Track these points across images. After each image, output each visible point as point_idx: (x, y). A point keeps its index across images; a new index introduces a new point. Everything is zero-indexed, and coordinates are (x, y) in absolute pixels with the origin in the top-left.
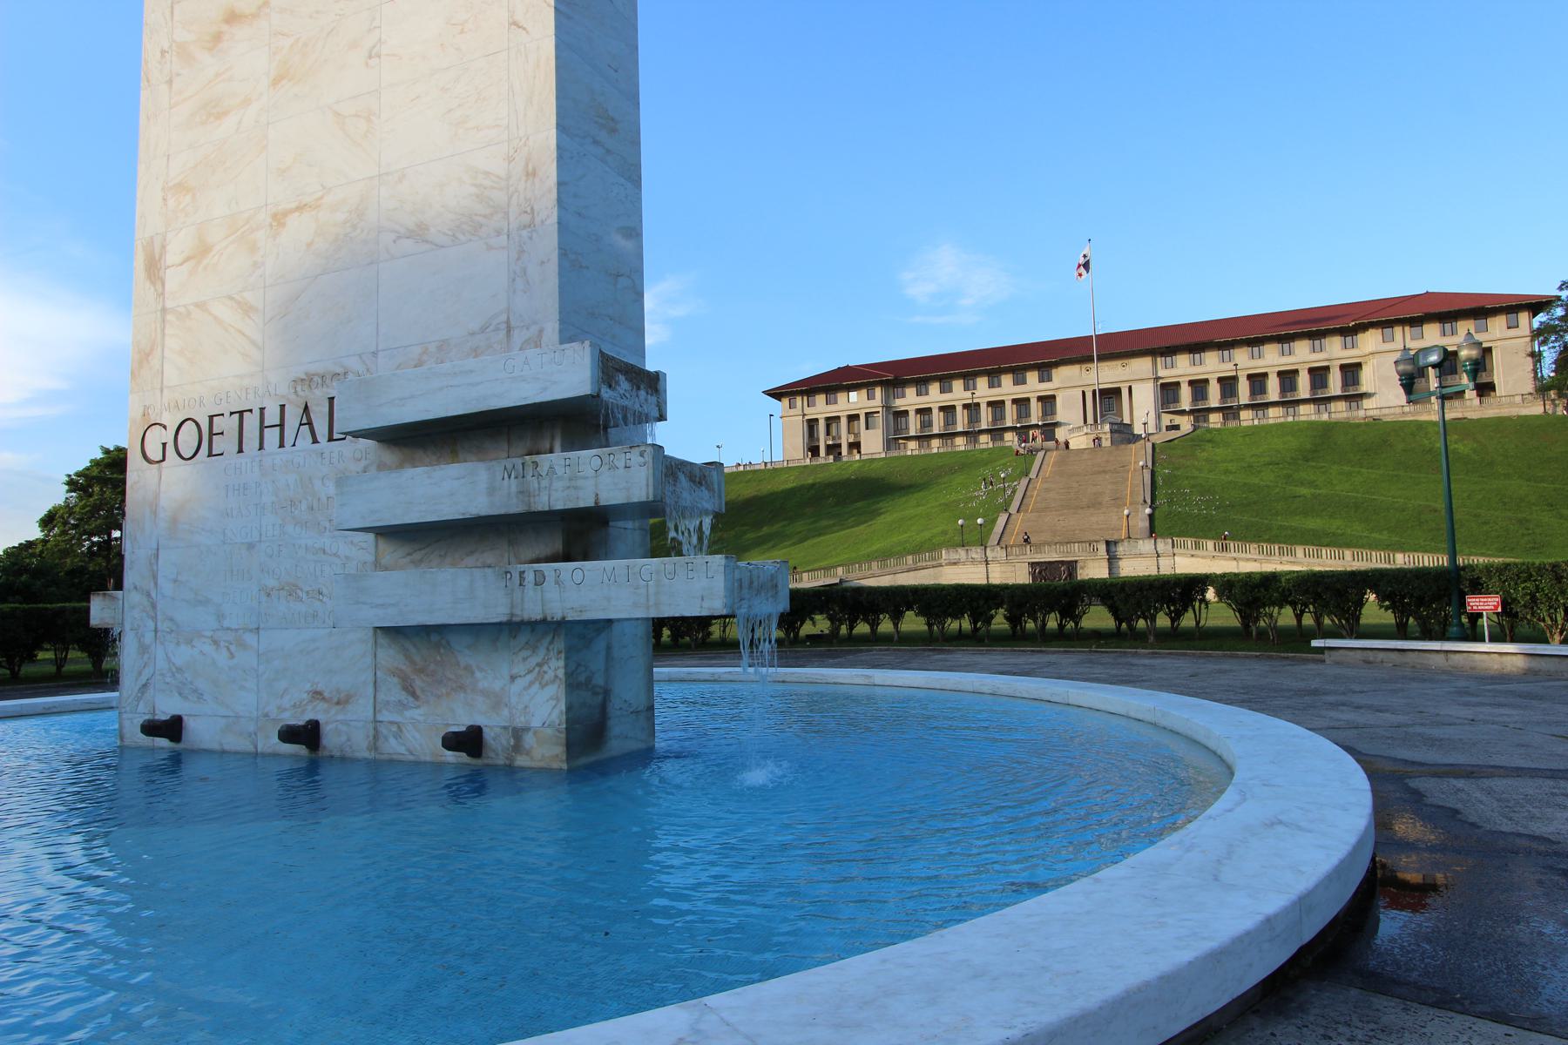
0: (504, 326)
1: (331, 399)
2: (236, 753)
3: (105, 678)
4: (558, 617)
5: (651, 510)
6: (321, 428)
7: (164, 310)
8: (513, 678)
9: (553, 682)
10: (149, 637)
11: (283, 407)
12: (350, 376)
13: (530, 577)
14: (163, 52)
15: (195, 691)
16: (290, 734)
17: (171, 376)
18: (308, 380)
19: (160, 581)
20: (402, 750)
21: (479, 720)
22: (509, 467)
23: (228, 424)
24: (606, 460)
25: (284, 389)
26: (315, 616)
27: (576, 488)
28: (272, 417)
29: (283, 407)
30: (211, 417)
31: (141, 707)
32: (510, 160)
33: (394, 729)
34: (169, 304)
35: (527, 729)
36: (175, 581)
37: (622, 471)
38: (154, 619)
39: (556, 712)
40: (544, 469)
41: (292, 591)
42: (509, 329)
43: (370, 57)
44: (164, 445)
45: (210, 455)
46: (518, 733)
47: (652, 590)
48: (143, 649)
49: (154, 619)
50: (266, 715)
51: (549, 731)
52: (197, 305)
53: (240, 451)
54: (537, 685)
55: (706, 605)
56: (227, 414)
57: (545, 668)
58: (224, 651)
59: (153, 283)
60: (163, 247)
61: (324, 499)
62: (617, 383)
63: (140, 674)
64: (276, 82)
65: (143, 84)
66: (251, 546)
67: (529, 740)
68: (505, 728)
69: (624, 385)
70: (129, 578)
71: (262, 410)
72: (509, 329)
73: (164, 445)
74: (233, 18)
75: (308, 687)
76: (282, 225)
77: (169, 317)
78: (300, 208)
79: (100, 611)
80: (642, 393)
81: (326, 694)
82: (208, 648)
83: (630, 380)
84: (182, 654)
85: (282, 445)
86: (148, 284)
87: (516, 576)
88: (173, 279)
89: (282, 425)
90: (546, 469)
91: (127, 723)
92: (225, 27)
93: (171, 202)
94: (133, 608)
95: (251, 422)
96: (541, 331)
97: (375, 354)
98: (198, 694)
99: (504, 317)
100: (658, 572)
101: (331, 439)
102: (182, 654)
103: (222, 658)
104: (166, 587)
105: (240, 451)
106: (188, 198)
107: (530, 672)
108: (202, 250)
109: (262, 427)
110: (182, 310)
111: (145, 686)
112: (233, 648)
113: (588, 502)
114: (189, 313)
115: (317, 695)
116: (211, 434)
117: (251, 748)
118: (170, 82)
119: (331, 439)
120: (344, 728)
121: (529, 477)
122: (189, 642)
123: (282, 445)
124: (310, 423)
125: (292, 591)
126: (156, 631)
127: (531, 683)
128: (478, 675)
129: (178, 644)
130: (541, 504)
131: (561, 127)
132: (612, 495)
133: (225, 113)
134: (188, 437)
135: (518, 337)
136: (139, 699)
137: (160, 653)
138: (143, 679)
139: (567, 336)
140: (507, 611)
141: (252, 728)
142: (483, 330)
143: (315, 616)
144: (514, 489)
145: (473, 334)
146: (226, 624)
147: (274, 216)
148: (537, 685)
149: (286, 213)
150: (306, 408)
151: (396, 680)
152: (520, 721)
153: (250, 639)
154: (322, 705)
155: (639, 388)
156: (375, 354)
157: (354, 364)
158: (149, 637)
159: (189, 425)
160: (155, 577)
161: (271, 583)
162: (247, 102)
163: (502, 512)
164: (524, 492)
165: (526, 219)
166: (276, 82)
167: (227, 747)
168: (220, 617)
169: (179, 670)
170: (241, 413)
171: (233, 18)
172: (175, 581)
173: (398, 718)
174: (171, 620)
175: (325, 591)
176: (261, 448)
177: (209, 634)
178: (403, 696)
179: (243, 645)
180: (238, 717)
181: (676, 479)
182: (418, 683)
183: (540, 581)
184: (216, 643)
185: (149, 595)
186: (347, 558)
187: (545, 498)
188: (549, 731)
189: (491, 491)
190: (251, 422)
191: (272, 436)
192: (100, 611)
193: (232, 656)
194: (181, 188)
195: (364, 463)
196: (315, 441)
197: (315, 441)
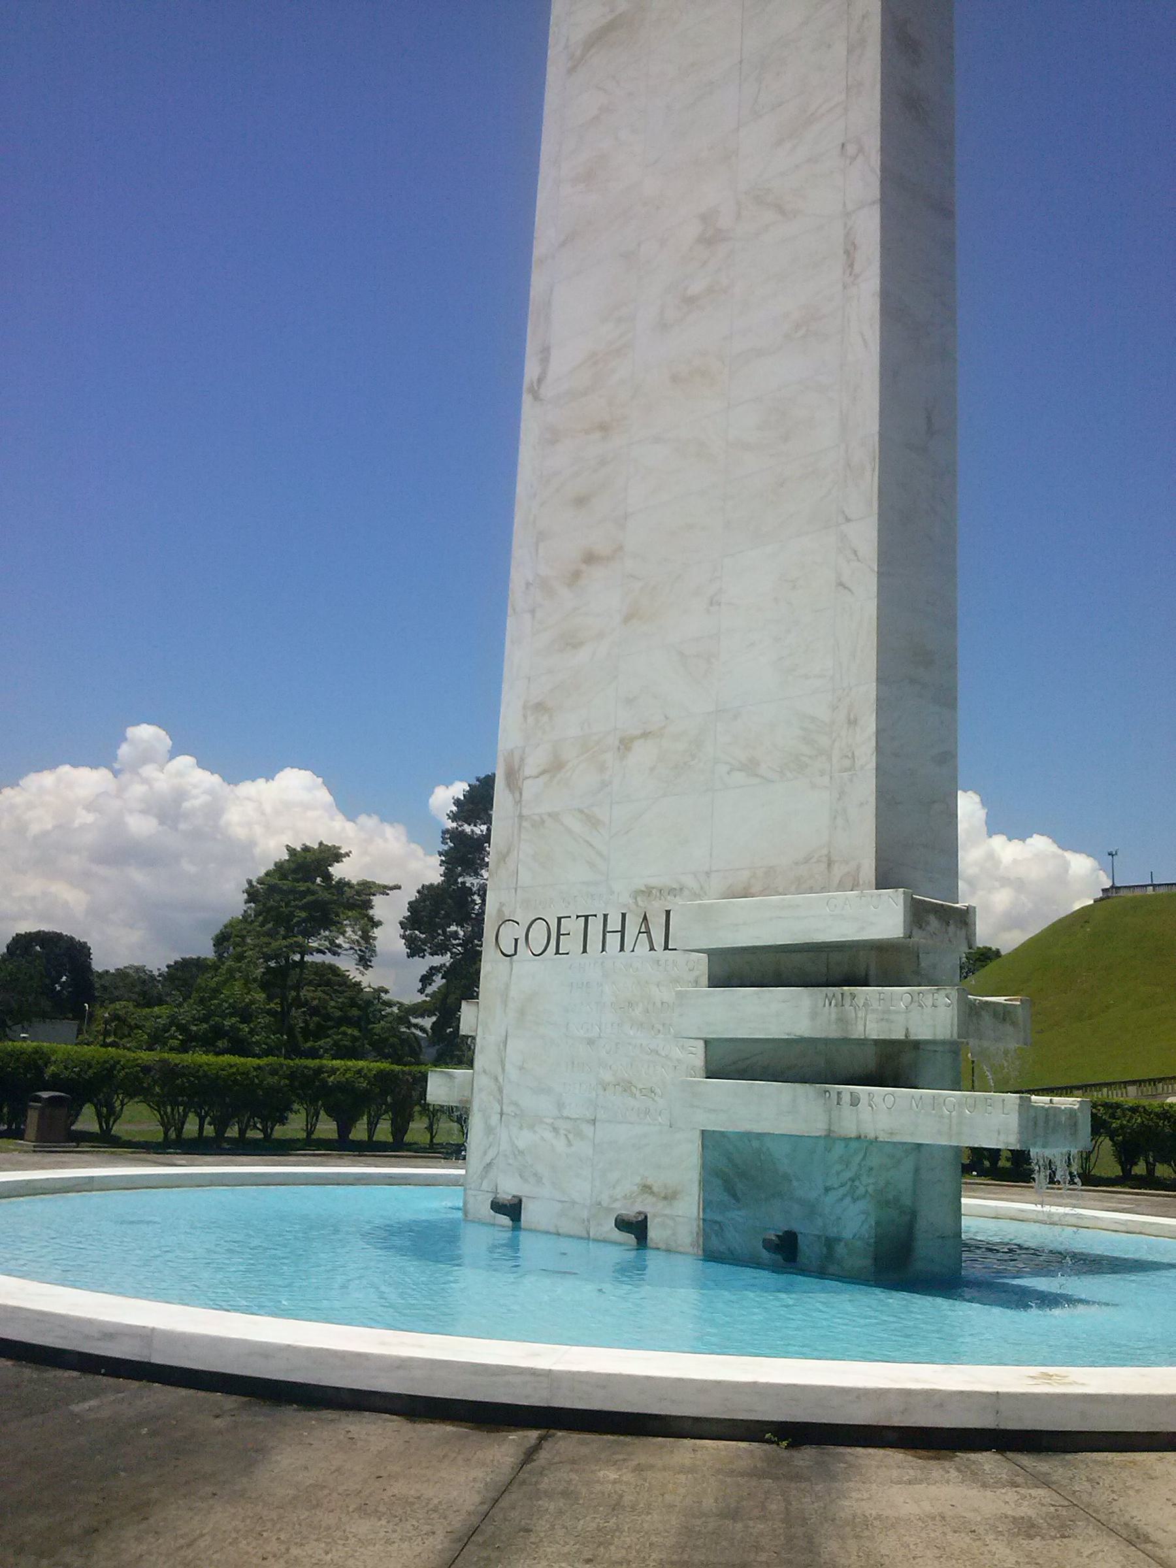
0: (825, 859)
1: (668, 913)
2: (570, 1236)
3: (456, 1152)
4: (872, 1135)
5: (954, 1048)
6: (658, 939)
7: (521, 816)
8: (827, 1190)
9: (864, 1196)
11: (624, 915)
12: (686, 893)
13: (846, 1098)
14: (528, 585)
15: (535, 1175)
16: (623, 1224)
17: (525, 877)
18: (648, 892)
19: (507, 1067)
20: (722, 1248)
21: (795, 1226)
22: (830, 995)
23: (574, 926)
24: (916, 998)
25: (626, 899)
26: (647, 1112)
27: (887, 1020)
28: (614, 924)
29: (624, 915)
30: (559, 919)
31: (485, 1186)
32: (834, 708)
33: (716, 1228)
34: (525, 812)
35: (838, 1240)
36: (521, 1068)
37: (928, 1010)
38: (501, 1103)
39: (866, 1226)
40: (860, 1001)
41: (627, 1087)
42: (830, 864)
43: (711, 604)
44: (516, 940)
45: (557, 953)
46: (830, 1243)
47: (954, 1121)
48: (489, 1130)
49: (501, 1103)
50: (600, 1204)
51: (859, 1243)
52: (550, 815)
53: (585, 951)
54: (848, 1199)
55: (1002, 1138)
57: (857, 1183)
58: (563, 1137)
59: (513, 793)
60: (522, 760)
61: (659, 1004)
62: (928, 923)
63: (485, 1153)
64: (627, 619)
65: (510, 611)
66: (591, 1042)
67: (840, 1250)
68: (819, 1237)
69: (934, 922)
70: (481, 1060)
71: (605, 916)
72: (830, 864)
73: (516, 940)
74: (590, 558)
75: (638, 1180)
76: (628, 749)
77: (524, 824)
78: (645, 735)
79: (440, 1087)
80: (951, 929)
81: (655, 1189)
82: (549, 1135)
83: (940, 918)
84: (524, 1139)
85: (622, 949)
86: (507, 791)
87: (834, 1096)
89: (623, 932)
90: (862, 1001)
91: (471, 1200)
92: (584, 567)
93: (531, 719)
94: (481, 1090)
95: (595, 926)
96: (859, 867)
97: (708, 874)
98: (539, 1179)
99: (825, 851)
100: (960, 1105)
101: (666, 948)
102: (524, 1139)
103: (560, 1145)
104: (513, 1073)
105: (585, 951)
106: (545, 718)
107: (842, 1185)
108: (556, 766)
110: (537, 818)
111: (489, 1165)
112: (571, 1136)
113: (899, 1035)
114: (543, 822)
115: (647, 1189)
116: (559, 934)
117: (584, 1234)
118: (533, 612)
119: (666, 948)
120: (671, 1223)
121: (847, 1006)
122: (532, 1127)
123: (622, 949)
124: (648, 932)
125: (627, 1087)
126: (502, 1114)
127: (845, 1196)
128: (795, 1183)
129: (521, 1128)
130: (857, 1032)
131: (880, 680)
132: (922, 1032)
133: (581, 644)
135: (838, 871)
136: (482, 1178)
138: (488, 1160)
139: (884, 881)
140: (826, 1127)
141: (585, 1214)
142: (807, 860)
143: (647, 1112)
144: (833, 1016)
145: (796, 864)
146: (566, 1113)
147: (622, 741)
148: (848, 1199)
149: (633, 739)
150: (645, 918)
151: (720, 1182)
152: (832, 1232)
153: (587, 1129)
154: (651, 1199)
155: (948, 924)
156: (708, 874)
157: (689, 881)
158: (494, 1120)
159: (539, 926)
160: (502, 1063)
161: (608, 1077)
163: (823, 1035)
164: (842, 1020)
165: (847, 763)
166: (627, 619)
167: (561, 1231)
168: (560, 1106)
169: (521, 1152)
170: (587, 917)
171: (590, 558)
172: (521, 1068)
173: (719, 1218)
174: (516, 1104)
175: (658, 1091)
177: (549, 1121)
178: (725, 1197)
179: (580, 1135)
180: (574, 1203)
181: (978, 1015)
182: (740, 1186)
183: (855, 1101)
184: (555, 1130)
185: (496, 1079)
186: (679, 1061)
187: (861, 1028)
188: (859, 1243)
189: (814, 1015)
190: (595, 926)
191: (613, 940)
192: (440, 1087)
193: (570, 1144)
194: (540, 707)
195: (696, 973)
196: (652, 949)
197: (652, 949)
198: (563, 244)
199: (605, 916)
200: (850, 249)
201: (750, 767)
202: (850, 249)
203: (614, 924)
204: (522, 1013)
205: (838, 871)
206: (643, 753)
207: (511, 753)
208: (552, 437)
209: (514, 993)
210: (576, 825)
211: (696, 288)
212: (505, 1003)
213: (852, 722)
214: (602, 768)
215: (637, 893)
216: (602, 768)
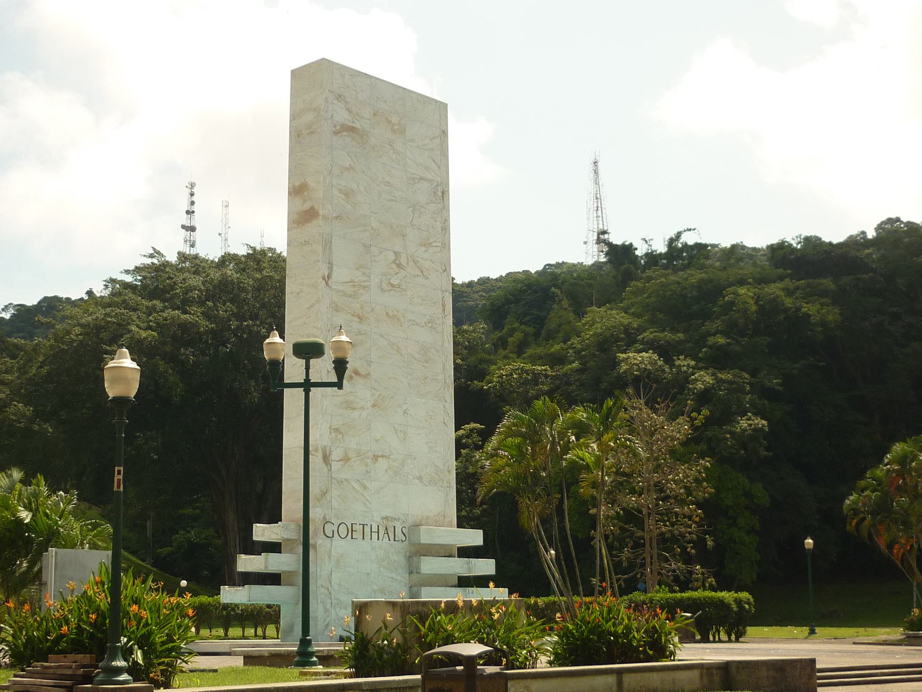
10: (328, 606)
18: (387, 518)
25: (379, 519)
28: (375, 529)
38: (331, 599)
48: (326, 610)
49: (331, 599)
64: (374, 406)
66: (368, 574)
78: (383, 456)
88: (335, 466)
93: (333, 434)
104: (336, 587)
106: (340, 436)
108: (346, 459)
111: (328, 625)
134: (343, 529)
135: (447, 520)
137: (333, 612)
149: (378, 456)
157: (402, 517)
158: (328, 606)
161: (376, 588)
162: (362, 408)
191: (375, 536)
194: (337, 430)
198: (336, 218)
200: (444, 305)
201: (420, 478)
202: (444, 305)
203: (375, 529)
204: (338, 561)
205: (447, 520)
206: (382, 464)
207: (325, 447)
208: (337, 309)
209: (333, 553)
210: (357, 486)
211: (395, 281)
212: (330, 557)
213: (449, 472)
214: (366, 465)
215: (383, 518)
216: (366, 465)
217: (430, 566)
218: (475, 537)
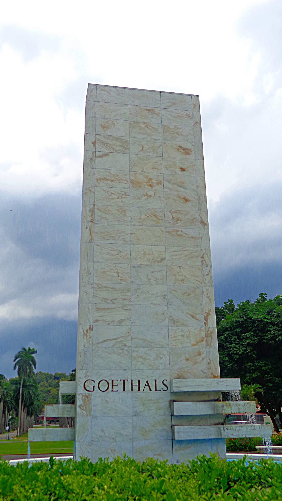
1: (156, 381)
11: (139, 381)
29: (139, 381)
30: (113, 381)
44: (94, 387)
45: (112, 391)
53: (124, 390)
56: (119, 380)
71: (132, 381)
73: (94, 387)
85: (139, 390)
101: (156, 390)
105: (124, 390)
109: (132, 385)
123: (139, 390)
124: (148, 385)
134: (103, 386)
150: (147, 382)
176: (132, 390)
196: (150, 390)
197: (150, 390)
199: (132, 381)
217: (182, 408)
218: (234, 384)
